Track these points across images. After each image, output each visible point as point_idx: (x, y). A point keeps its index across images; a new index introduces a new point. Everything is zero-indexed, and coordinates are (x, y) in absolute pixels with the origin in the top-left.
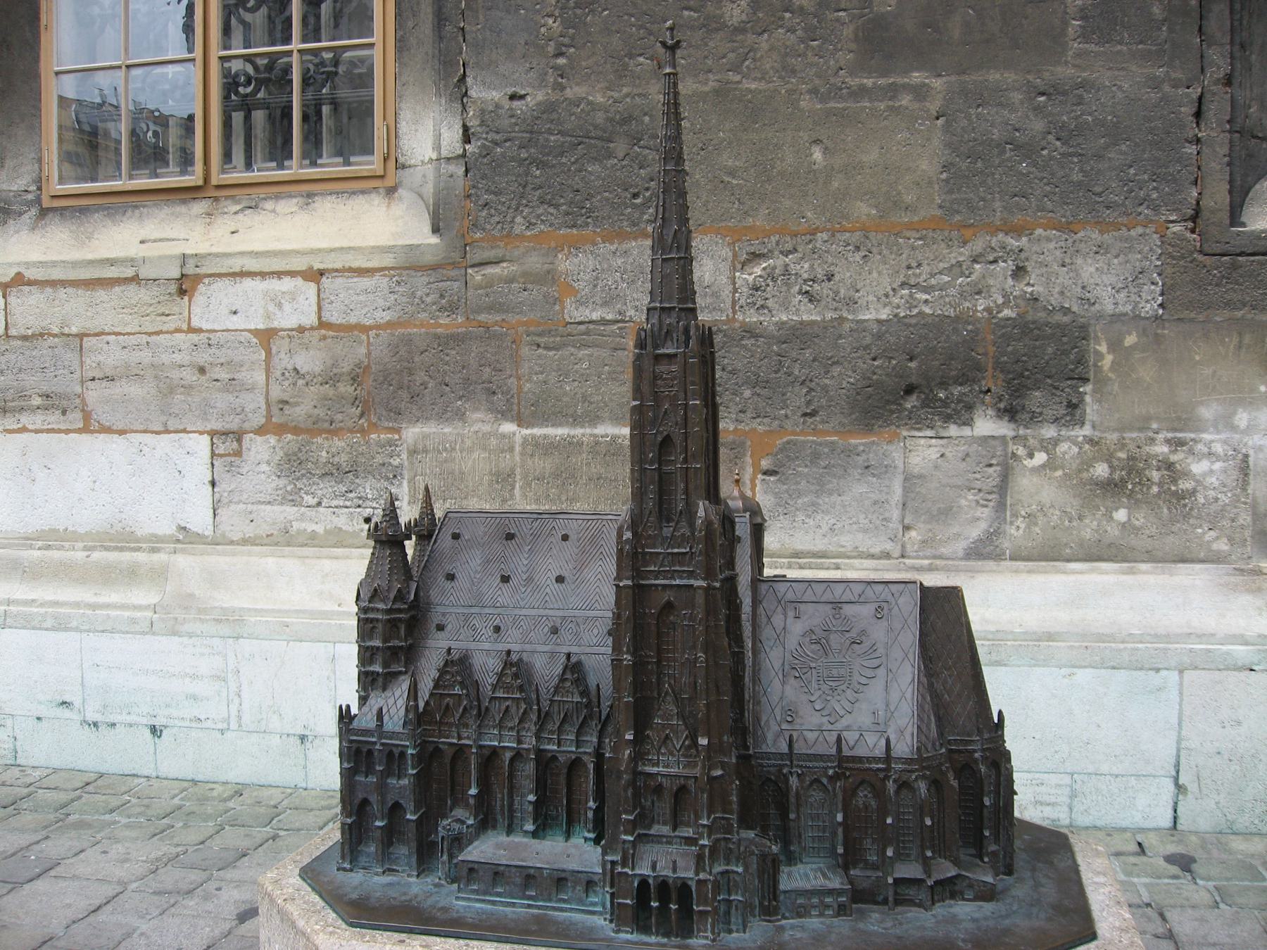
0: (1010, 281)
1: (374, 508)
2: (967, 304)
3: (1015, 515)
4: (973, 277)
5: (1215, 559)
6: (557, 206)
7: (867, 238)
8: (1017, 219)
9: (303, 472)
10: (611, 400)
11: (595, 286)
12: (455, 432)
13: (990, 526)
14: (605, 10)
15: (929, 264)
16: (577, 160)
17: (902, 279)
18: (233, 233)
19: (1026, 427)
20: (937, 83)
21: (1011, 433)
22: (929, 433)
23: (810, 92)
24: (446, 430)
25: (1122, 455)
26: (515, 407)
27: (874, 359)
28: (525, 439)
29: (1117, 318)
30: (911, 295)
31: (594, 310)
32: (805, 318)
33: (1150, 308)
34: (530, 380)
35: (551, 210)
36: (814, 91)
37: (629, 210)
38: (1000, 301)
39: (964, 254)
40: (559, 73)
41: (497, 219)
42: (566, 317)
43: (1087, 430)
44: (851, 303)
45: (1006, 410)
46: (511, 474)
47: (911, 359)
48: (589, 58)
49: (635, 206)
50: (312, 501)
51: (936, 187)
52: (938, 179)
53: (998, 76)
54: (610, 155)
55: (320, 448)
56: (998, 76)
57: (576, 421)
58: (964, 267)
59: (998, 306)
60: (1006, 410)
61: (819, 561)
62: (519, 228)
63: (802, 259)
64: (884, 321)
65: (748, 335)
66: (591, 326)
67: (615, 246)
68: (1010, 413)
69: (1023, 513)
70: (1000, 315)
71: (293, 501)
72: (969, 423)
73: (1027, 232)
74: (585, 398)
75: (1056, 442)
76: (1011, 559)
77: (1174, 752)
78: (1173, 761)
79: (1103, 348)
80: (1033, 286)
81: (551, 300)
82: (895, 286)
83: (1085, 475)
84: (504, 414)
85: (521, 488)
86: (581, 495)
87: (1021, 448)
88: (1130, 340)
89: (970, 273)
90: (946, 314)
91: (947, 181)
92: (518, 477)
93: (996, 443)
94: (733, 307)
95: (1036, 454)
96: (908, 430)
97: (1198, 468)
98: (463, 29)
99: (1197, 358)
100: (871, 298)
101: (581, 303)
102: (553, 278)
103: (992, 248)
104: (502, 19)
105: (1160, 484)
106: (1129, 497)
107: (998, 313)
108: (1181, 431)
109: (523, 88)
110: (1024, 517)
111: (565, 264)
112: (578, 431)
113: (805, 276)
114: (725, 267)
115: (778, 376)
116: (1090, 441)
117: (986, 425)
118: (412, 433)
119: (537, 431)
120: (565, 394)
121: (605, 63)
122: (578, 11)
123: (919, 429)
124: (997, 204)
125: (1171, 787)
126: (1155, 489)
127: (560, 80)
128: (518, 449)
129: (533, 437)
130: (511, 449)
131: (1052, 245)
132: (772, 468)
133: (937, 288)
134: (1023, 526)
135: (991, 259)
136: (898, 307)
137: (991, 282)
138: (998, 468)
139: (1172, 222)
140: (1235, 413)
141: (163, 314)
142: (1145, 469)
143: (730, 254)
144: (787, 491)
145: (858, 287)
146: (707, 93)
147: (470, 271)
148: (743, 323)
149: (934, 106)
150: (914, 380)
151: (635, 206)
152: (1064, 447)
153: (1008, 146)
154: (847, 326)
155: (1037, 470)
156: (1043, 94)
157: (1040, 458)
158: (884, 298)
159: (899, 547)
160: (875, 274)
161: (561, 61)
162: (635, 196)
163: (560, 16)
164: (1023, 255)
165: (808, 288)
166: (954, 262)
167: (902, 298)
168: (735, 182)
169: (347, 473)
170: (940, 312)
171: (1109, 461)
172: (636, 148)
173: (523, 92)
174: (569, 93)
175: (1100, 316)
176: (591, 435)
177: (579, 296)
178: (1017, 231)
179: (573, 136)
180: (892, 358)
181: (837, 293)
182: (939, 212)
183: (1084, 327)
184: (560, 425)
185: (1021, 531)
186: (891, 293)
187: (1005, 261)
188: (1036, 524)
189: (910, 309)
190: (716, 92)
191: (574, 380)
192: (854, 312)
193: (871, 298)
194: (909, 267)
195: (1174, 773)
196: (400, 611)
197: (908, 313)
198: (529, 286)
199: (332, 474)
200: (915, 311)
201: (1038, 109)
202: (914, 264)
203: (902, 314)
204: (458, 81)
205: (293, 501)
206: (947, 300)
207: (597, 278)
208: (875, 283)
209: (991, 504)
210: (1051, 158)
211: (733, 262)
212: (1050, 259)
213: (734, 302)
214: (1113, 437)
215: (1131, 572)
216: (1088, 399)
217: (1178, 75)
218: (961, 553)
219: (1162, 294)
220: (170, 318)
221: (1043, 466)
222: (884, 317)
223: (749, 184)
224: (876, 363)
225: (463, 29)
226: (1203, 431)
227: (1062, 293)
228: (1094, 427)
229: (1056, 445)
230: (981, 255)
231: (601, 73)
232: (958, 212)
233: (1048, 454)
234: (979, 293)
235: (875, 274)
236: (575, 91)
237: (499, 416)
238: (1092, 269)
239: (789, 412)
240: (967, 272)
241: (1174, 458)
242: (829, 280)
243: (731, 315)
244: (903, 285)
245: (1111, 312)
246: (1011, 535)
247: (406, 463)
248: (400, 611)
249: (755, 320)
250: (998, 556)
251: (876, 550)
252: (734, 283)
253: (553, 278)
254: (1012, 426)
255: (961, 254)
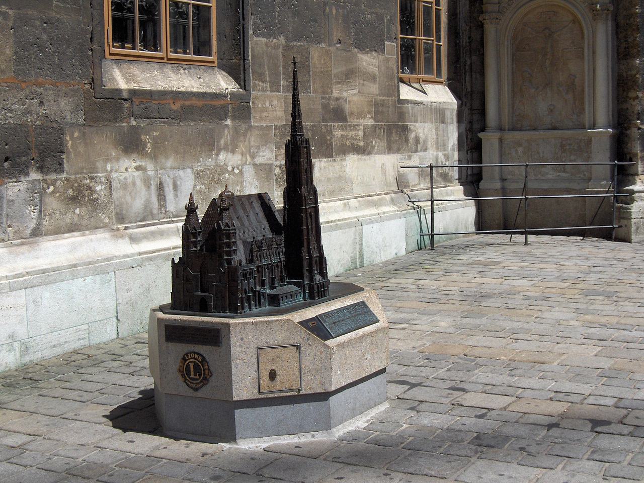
5: (105, 226)
8: (40, 80)
13: (37, 222)
20: (11, 12)
21: (42, 178)
22: (15, 180)
25: (76, 185)
29: (72, 124)
33: (81, 121)
39: (22, 95)
43: (64, 175)
47: (6, 145)
68: (41, 169)
72: (27, 174)
75: (56, 181)
76: (45, 235)
77: (115, 306)
78: (115, 310)
79: (68, 138)
83: (66, 195)
88: (76, 134)
89: (25, 104)
90: (18, 123)
93: (36, 182)
95: (50, 186)
96: (7, 179)
97: (98, 188)
99: (95, 142)
105: (88, 197)
106: (79, 203)
108: (93, 173)
116: (67, 179)
117: (34, 175)
123: (11, 178)
125: (116, 321)
126: (87, 199)
131: (51, 92)
135: (32, 98)
139: (86, 84)
140: (106, 165)
142: (83, 190)
149: (10, 24)
150: (8, 155)
152: (59, 182)
156: (45, 23)
157: (52, 188)
159: (7, 236)
164: (42, 96)
171: (72, 188)
175: (67, 124)
178: (40, 85)
182: (13, 74)
183: (62, 129)
187: (36, 99)
195: (116, 315)
201: (44, 29)
203: (3, 123)
210: (49, 53)
212: (50, 98)
214: (73, 177)
215: (84, 235)
216: (65, 161)
217: (85, 20)
218: (28, 236)
219: (84, 115)
226: (97, 172)
227: (55, 114)
228: (67, 173)
229: (56, 182)
230: (28, 96)
234: (28, 113)
238: (64, 104)
241: (91, 185)
245: (70, 123)
250: (41, 235)
254: (42, 174)
255: (22, 95)
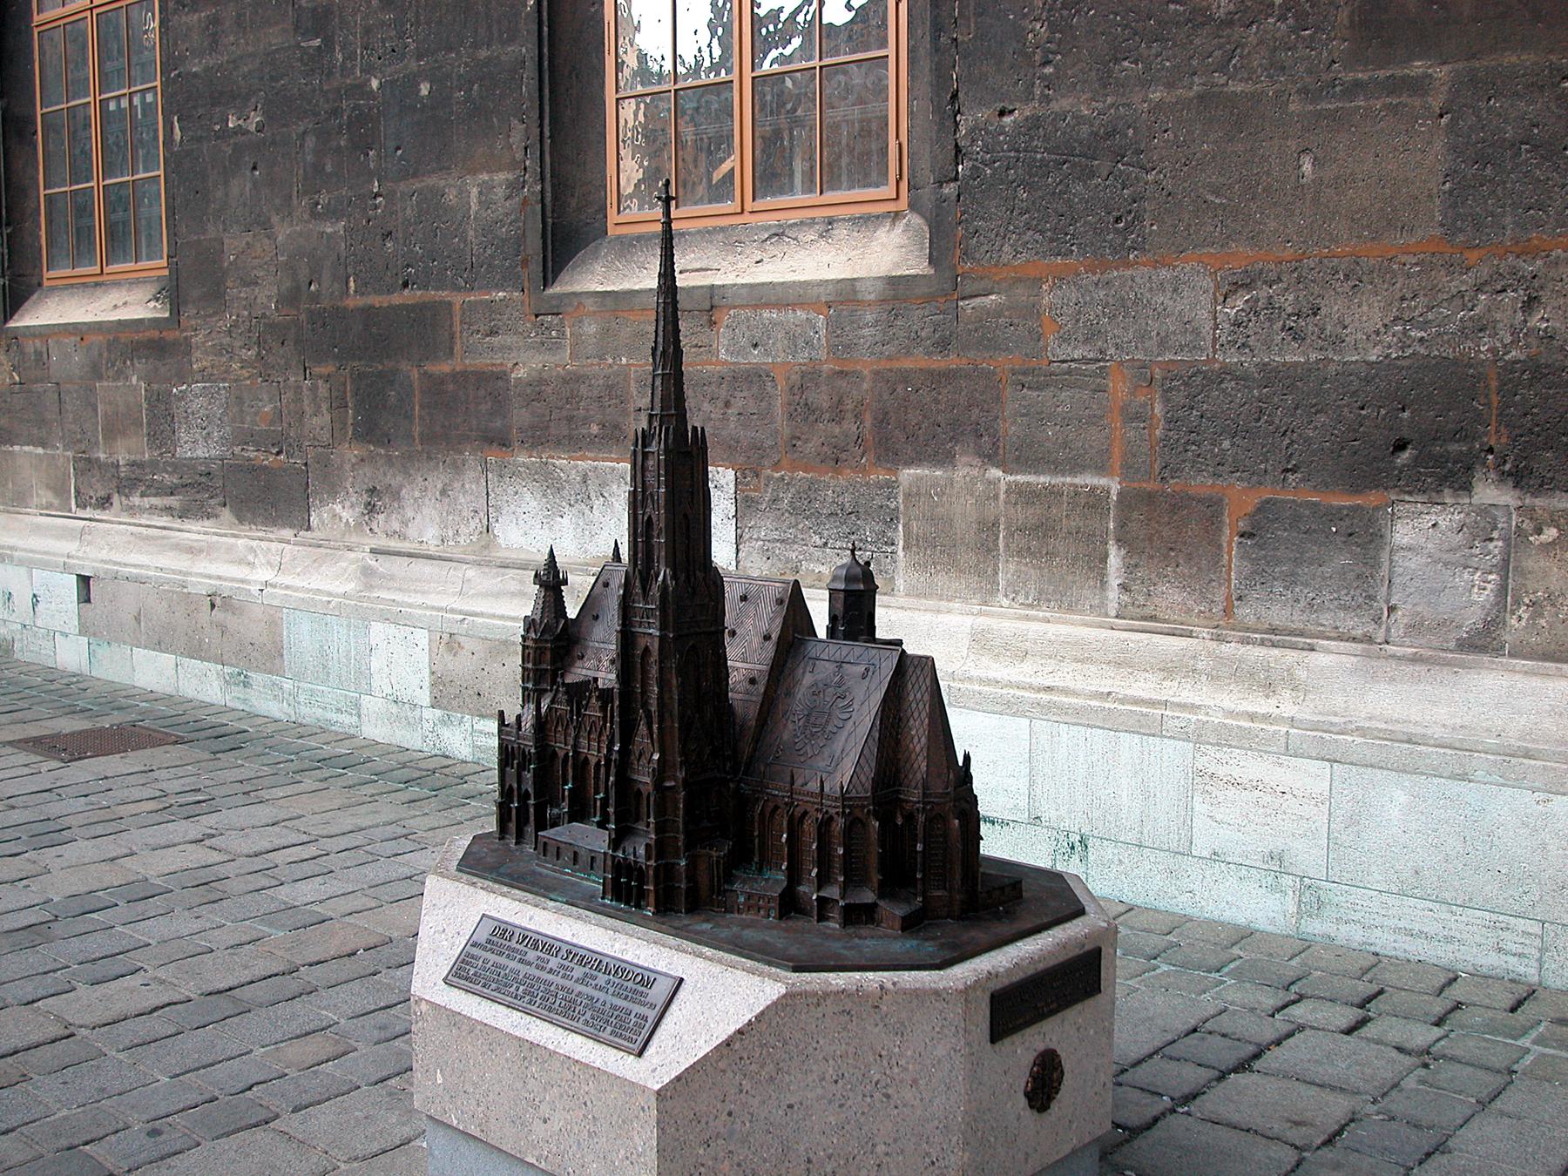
0: (1520, 316)
1: (873, 552)
2: (1469, 344)
3: (1517, 602)
4: (1477, 310)
6: (1042, 232)
7: (1358, 263)
9: (813, 510)
10: (1091, 446)
11: (1078, 321)
12: (945, 476)
14: (1090, 10)
15: (1425, 295)
16: (1061, 181)
17: (1395, 312)
18: (757, 262)
19: (1534, 495)
20: (1441, 73)
23: (1299, 92)
24: (937, 473)
26: (1001, 451)
27: (1362, 408)
28: (1009, 484)
30: (1405, 332)
31: (1075, 348)
32: (1287, 359)
34: (1014, 422)
35: (1037, 236)
36: (1304, 91)
37: (1111, 236)
38: (1508, 340)
40: (1046, 84)
41: (986, 248)
42: (1049, 354)
44: (1338, 342)
45: (1510, 474)
46: (996, 524)
48: (1074, 66)
49: (1117, 231)
50: (819, 542)
51: (1437, 202)
52: (1439, 190)
53: (1514, 59)
54: (1092, 175)
55: (827, 487)
56: (1514, 59)
57: (1056, 467)
58: (1466, 298)
59: (1505, 346)
60: (1510, 474)
61: (1294, 639)
62: (1005, 258)
63: (1286, 289)
64: (1373, 363)
65: (1229, 377)
66: (1073, 365)
67: (1098, 276)
69: (1527, 600)
70: (1506, 358)
71: (803, 539)
72: (1467, 488)
73: (1543, 254)
74: (1065, 445)
76: (1511, 655)
80: (1548, 321)
81: (1035, 336)
82: (1386, 321)
84: (991, 457)
85: (1004, 537)
86: (1061, 549)
87: (1527, 521)
89: (1474, 306)
90: (1444, 355)
91: (1451, 192)
92: (1002, 527)
94: (1213, 347)
95: (1545, 530)
96: (1398, 494)
98: (956, 39)
100: (1359, 335)
101: (1064, 340)
102: (1038, 312)
103: (1501, 275)
104: (991, 26)
107: (1504, 354)
109: (1011, 104)
110: (1528, 606)
111: (1048, 298)
112: (1058, 480)
113: (1289, 310)
114: (1205, 299)
115: (1259, 424)
117: (1490, 493)
118: (908, 474)
119: (1020, 478)
120: (1048, 438)
121: (1090, 70)
122: (1065, 13)
124: (1509, 219)
127: (1047, 92)
128: (1002, 496)
129: (1017, 484)
130: (996, 497)
132: (1249, 529)
133: (1435, 324)
134: (1525, 616)
135: (1499, 288)
136: (1389, 347)
137: (1498, 316)
138: (1500, 544)
141: (696, 346)
143: (1212, 285)
144: (1265, 557)
145: (1346, 323)
146: (1191, 100)
147: (961, 303)
148: (1224, 365)
149: (1436, 104)
150: (1406, 433)
151: (1117, 231)
153: (1523, 147)
154: (1332, 368)
155: (1547, 547)
158: (1374, 336)
160: (1365, 308)
161: (1049, 70)
162: (1118, 220)
163: (1048, 19)
164: (1536, 283)
165: (1292, 324)
166: (1454, 291)
167: (1394, 336)
168: (1218, 201)
169: (850, 513)
170: (1436, 353)
172: (1120, 165)
173: (1011, 108)
174: (1055, 106)
176: (1071, 485)
177: (1062, 331)
178: (1530, 252)
179: (1058, 154)
180: (1381, 407)
181: (1322, 330)
182: (1438, 232)
184: (1043, 473)
185: (1523, 623)
186: (1383, 330)
188: (1541, 615)
189: (1402, 349)
190: (1201, 97)
191: (1055, 424)
192: (1340, 352)
193: (1359, 335)
194: (1403, 299)
196: (547, 641)
197: (1400, 354)
198: (1016, 321)
199: (837, 514)
200: (1409, 351)
202: (1409, 296)
203: (1394, 356)
204: (951, 98)
205: (803, 539)
206: (1445, 338)
207: (1080, 312)
208: (1365, 318)
209: (1489, 586)
211: (1214, 294)
213: (1215, 340)
220: (702, 349)
221: (1553, 543)
222: (1374, 358)
223: (1232, 204)
224: (1363, 412)
225: (956, 39)
230: (1486, 283)
231: (1086, 81)
232: (1461, 230)
233: (1559, 530)
235: (1365, 308)
236: (1063, 104)
237: (986, 460)
239: (1269, 468)
240: (1470, 305)
242: (1315, 314)
243: (1211, 355)
244: (1396, 319)
246: (1511, 626)
247: (902, 507)
248: (547, 641)
249: (1236, 360)
250: (1498, 651)
251: (1359, 632)
252: (1215, 318)
253: (1038, 312)
254: (1517, 493)
